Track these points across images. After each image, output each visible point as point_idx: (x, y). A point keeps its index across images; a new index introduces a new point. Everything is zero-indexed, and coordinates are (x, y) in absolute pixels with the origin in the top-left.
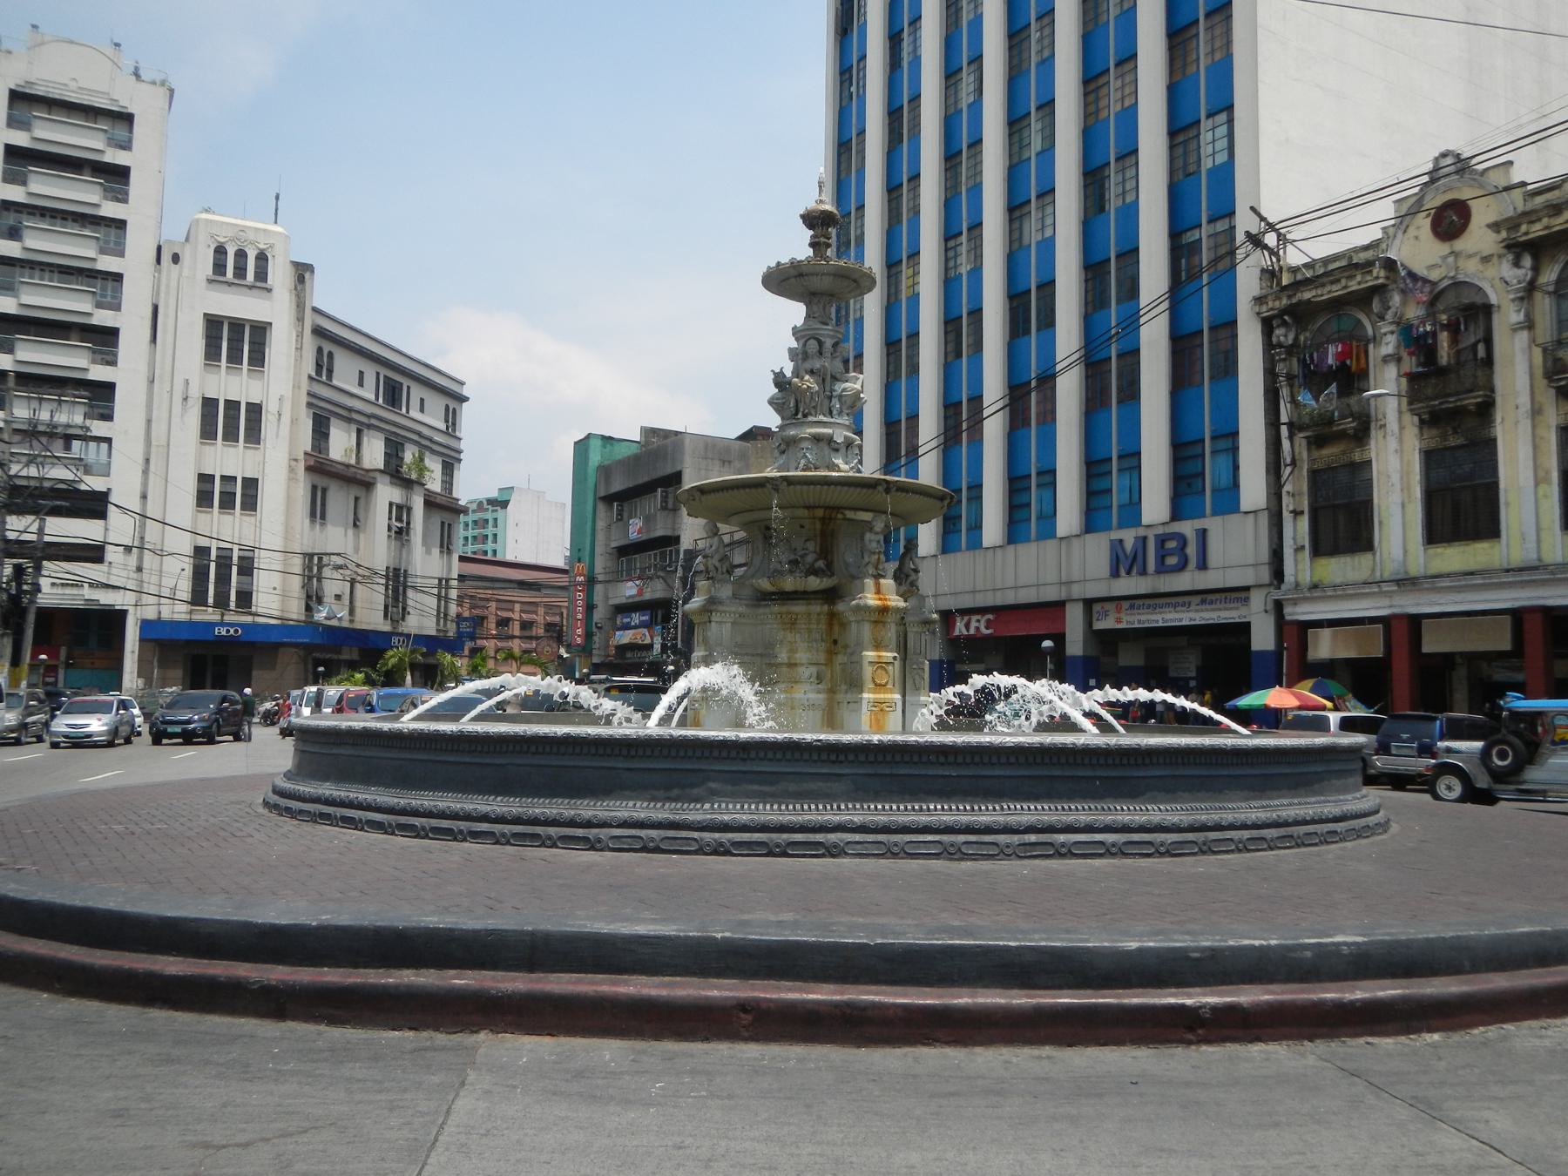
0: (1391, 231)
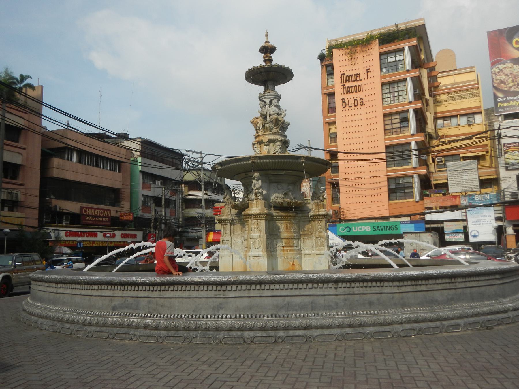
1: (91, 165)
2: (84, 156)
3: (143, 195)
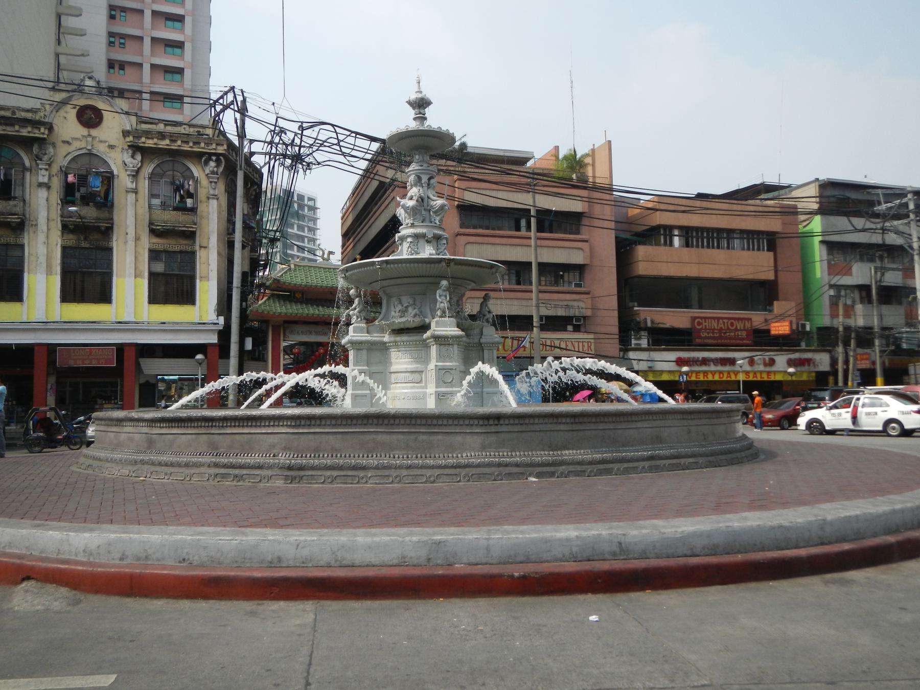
0: (47, 107)
1: (708, 247)
2: (691, 235)
3: (832, 286)
